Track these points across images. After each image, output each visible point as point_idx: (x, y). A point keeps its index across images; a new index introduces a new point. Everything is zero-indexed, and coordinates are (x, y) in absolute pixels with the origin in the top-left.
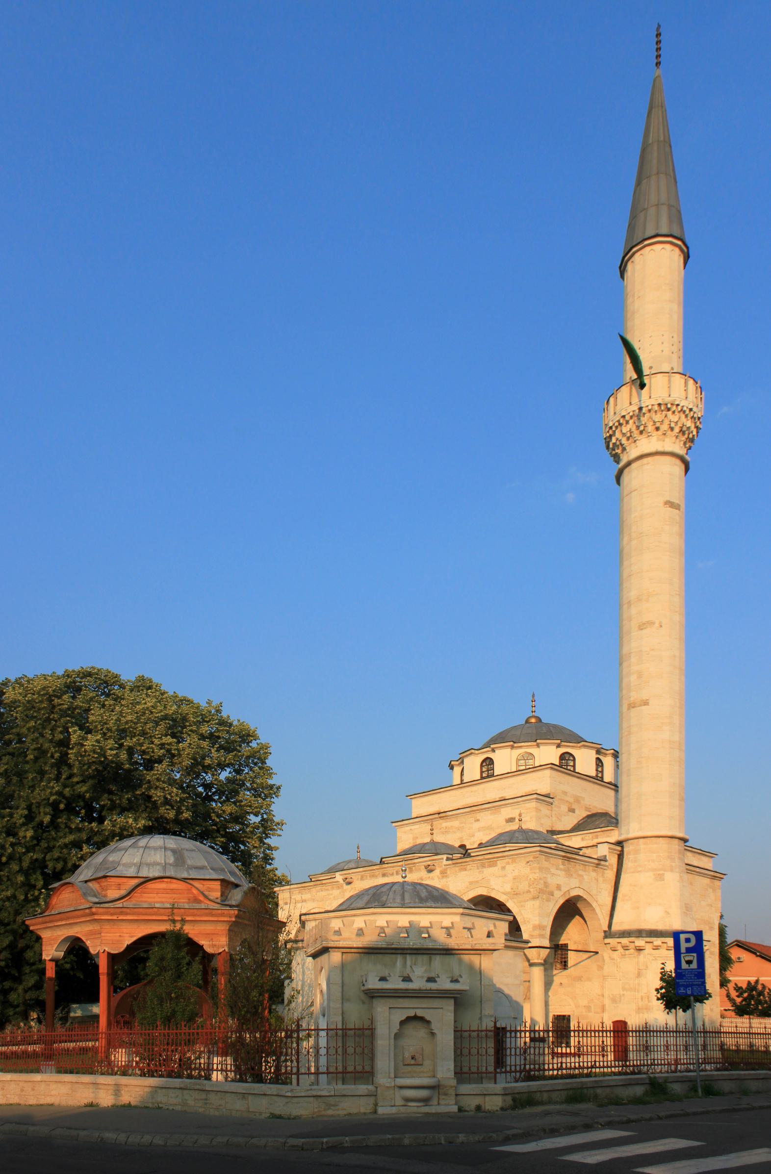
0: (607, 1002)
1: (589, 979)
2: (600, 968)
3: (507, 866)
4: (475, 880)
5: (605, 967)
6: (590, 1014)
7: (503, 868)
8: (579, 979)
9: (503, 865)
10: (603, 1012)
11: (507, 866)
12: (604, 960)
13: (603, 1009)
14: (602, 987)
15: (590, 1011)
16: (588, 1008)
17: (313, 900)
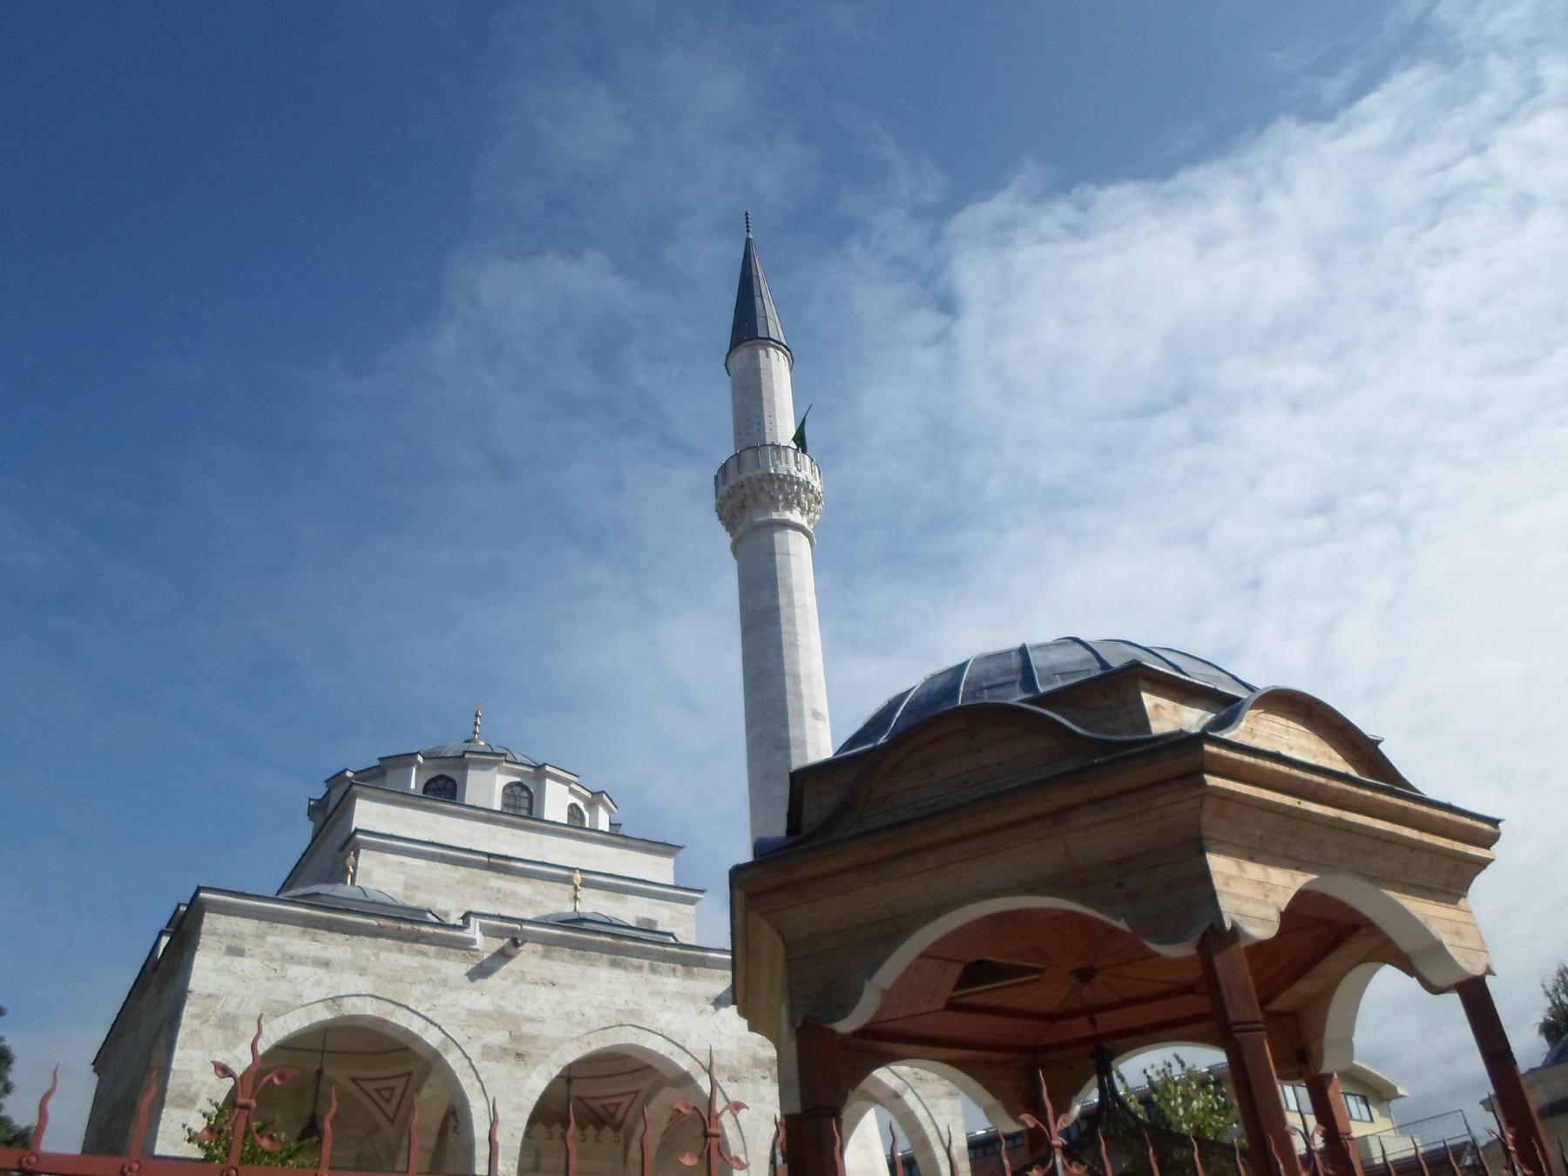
17: (362, 971)
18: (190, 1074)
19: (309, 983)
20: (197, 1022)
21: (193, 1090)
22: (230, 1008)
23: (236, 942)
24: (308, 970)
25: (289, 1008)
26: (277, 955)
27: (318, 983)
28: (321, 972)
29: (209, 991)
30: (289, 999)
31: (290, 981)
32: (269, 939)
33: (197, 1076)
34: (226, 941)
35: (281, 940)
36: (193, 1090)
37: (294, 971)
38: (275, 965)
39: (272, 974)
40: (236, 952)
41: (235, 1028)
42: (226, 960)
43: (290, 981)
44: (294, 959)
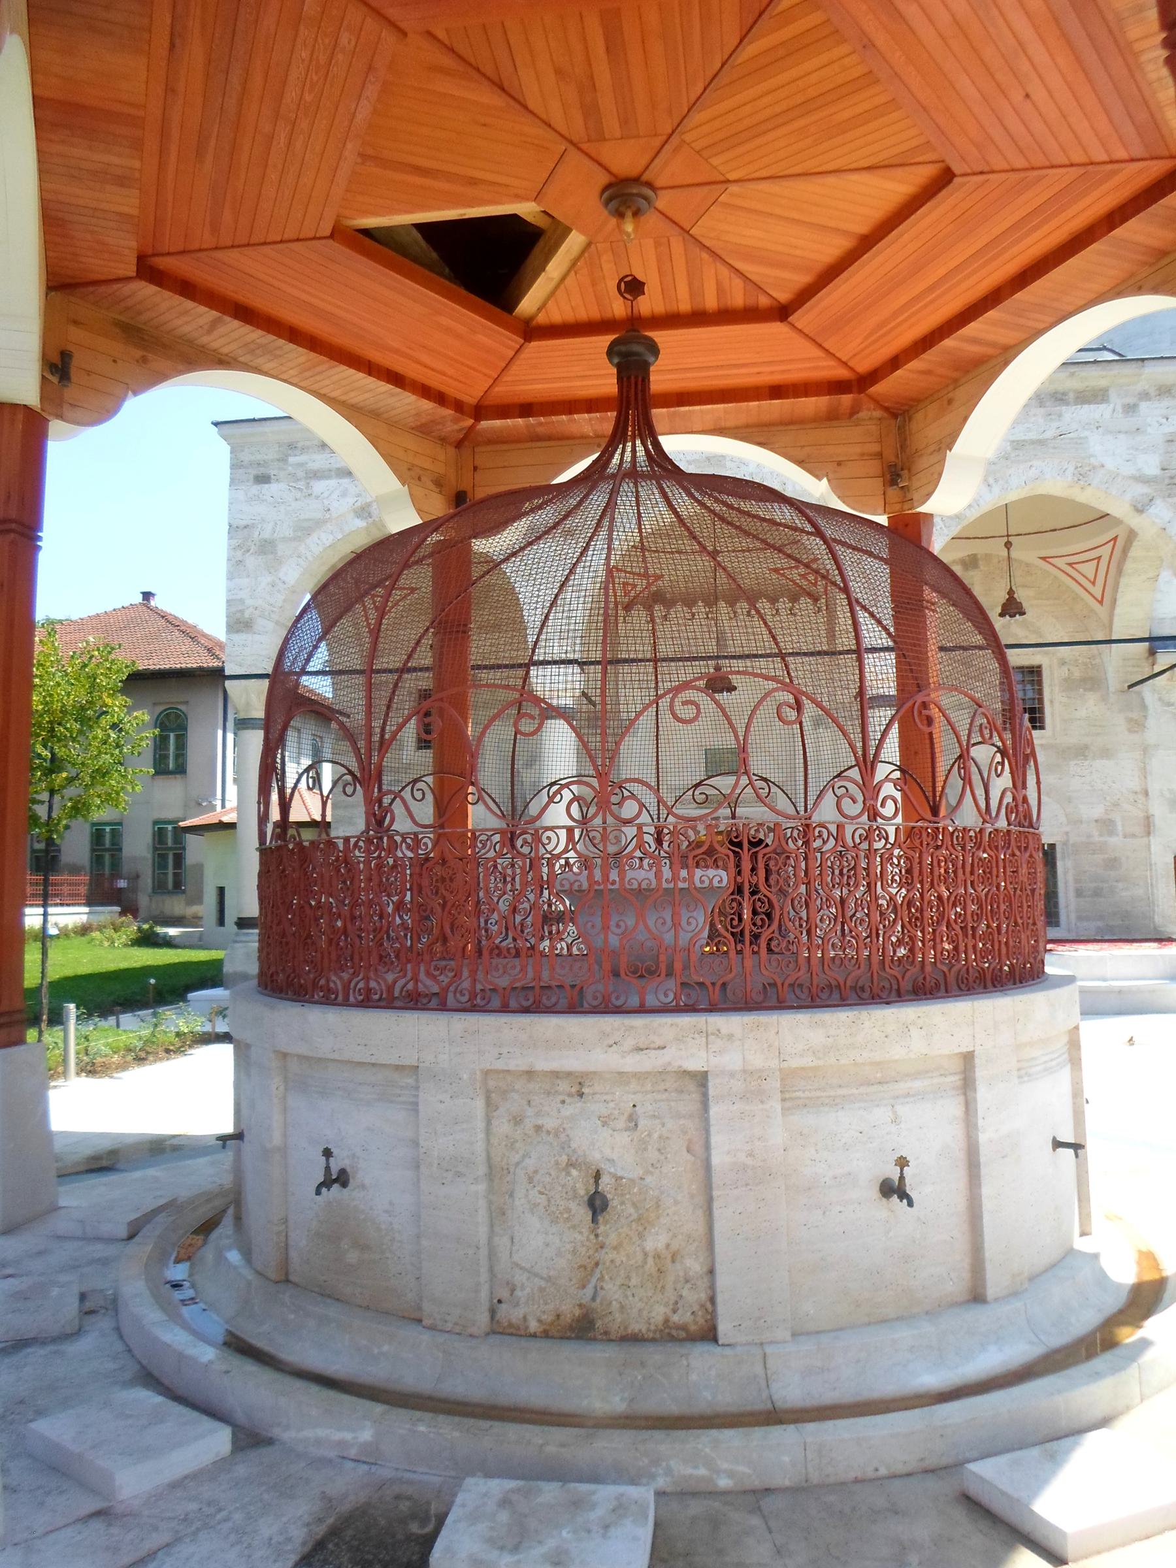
0: (1158, 809)
1: (1106, 753)
2: (1137, 725)
3: (1144, 406)
4: (1033, 436)
5: (1151, 722)
6: (1113, 840)
7: (1130, 409)
8: (1081, 752)
9: (1130, 400)
10: (1149, 834)
11: (1144, 406)
12: (1144, 707)
13: (1148, 825)
14: (1144, 773)
15: (1112, 833)
16: (1107, 825)
18: (242, 601)
19: (335, 496)
20: (239, 553)
21: (247, 615)
22: (266, 535)
23: (262, 470)
24: (332, 483)
25: (319, 524)
26: (300, 473)
27: (344, 494)
28: (345, 481)
29: (244, 523)
30: (318, 515)
31: (317, 497)
32: (291, 460)
33: (249, 602)
34: (253, 472)
35: (302, 458)
36: (247, 615)
37: (319, 486)
38: (301, 485)
39: (299, 495)
40: (263, 479)
41: (274, 552)
42: (255, 489)
43: (317, 497)
44: (317, 475)
